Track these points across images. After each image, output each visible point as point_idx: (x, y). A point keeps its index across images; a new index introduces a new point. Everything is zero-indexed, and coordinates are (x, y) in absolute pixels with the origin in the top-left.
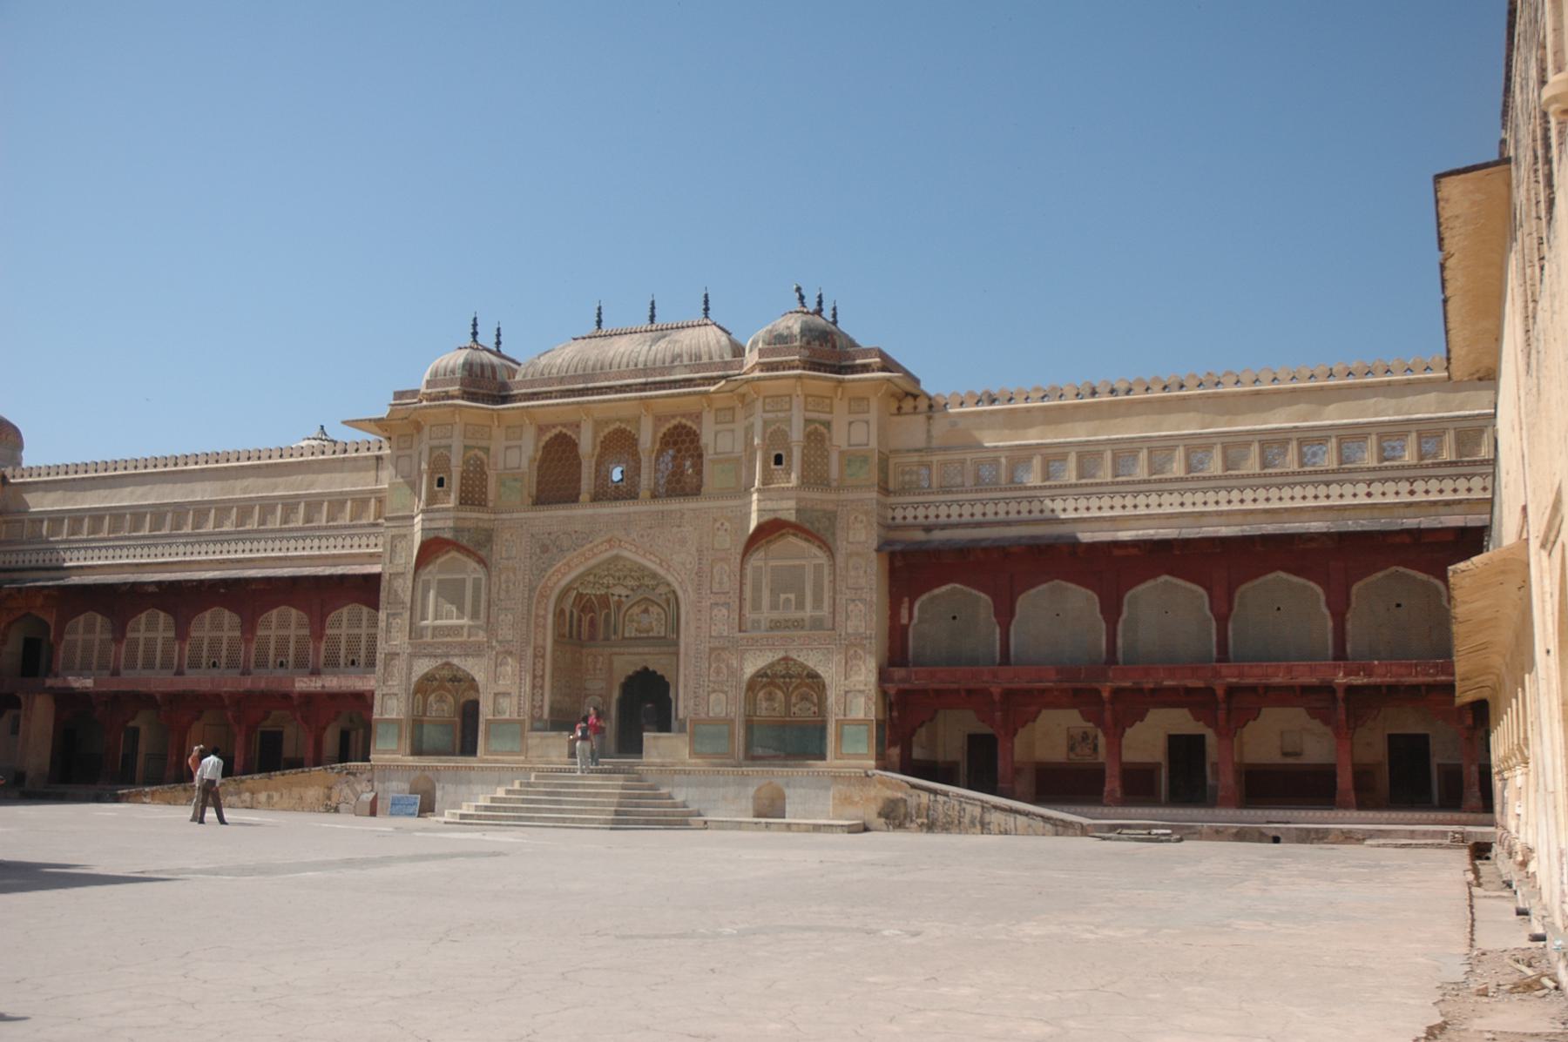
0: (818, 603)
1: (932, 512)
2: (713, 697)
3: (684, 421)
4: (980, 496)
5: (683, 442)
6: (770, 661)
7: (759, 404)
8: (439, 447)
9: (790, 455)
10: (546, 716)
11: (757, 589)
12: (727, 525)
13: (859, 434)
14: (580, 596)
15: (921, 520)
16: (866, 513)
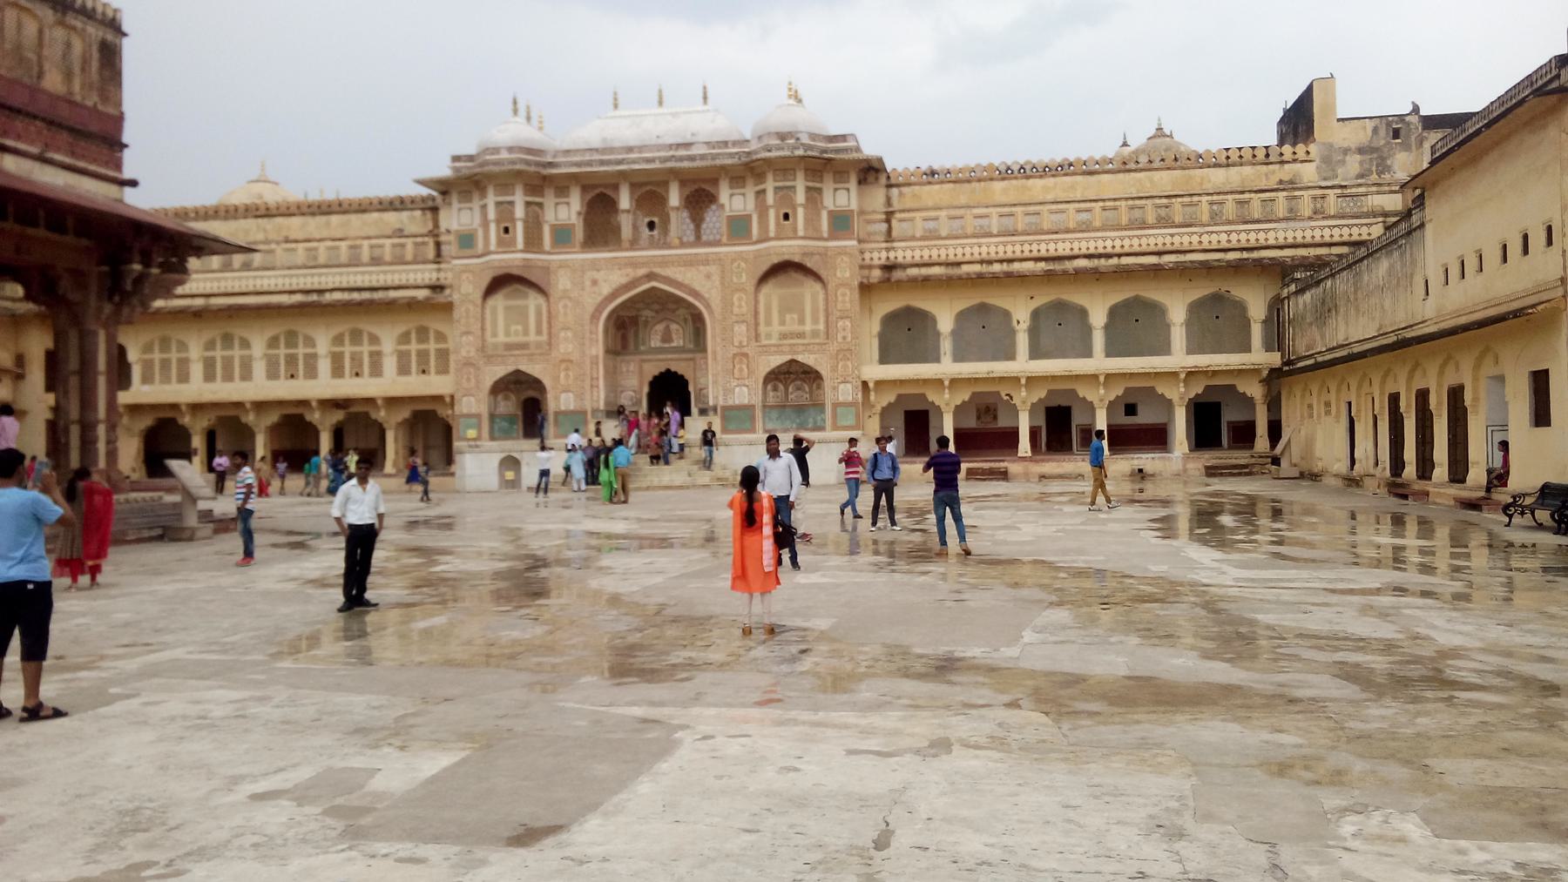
0: (815, 321)
7: (770, 177)
10: (602, 407)
14: (618, 317)
15: (883, 262)
16: (851, 255)
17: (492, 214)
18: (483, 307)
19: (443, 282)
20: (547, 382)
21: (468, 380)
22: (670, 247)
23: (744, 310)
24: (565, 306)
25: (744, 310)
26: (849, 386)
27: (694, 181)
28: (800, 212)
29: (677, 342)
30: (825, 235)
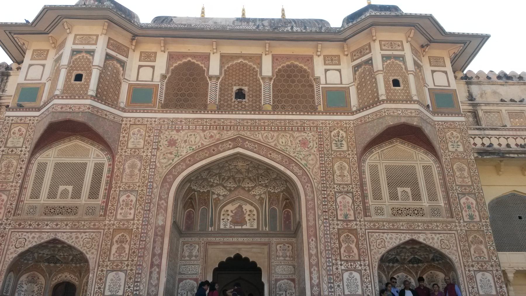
0: (432, 196)
2: (346, 275)
4: (519, 133)
5: (295, 76)
7: (376, 47)
8: (79, 52)
9: (407, 82)
11: (375, 181)
12: (341, 132)
14: (190, 189)
15: (479, 146)
16: (461, 131)
17: (65, 61)
20: (91, 257)
22: (259, 110)
23: (348, 179)
24: (133, 166)
25: (348, 179)
26: (488, 276)
27: (288, 57)
28: (411, 78)
29: (250, 224)
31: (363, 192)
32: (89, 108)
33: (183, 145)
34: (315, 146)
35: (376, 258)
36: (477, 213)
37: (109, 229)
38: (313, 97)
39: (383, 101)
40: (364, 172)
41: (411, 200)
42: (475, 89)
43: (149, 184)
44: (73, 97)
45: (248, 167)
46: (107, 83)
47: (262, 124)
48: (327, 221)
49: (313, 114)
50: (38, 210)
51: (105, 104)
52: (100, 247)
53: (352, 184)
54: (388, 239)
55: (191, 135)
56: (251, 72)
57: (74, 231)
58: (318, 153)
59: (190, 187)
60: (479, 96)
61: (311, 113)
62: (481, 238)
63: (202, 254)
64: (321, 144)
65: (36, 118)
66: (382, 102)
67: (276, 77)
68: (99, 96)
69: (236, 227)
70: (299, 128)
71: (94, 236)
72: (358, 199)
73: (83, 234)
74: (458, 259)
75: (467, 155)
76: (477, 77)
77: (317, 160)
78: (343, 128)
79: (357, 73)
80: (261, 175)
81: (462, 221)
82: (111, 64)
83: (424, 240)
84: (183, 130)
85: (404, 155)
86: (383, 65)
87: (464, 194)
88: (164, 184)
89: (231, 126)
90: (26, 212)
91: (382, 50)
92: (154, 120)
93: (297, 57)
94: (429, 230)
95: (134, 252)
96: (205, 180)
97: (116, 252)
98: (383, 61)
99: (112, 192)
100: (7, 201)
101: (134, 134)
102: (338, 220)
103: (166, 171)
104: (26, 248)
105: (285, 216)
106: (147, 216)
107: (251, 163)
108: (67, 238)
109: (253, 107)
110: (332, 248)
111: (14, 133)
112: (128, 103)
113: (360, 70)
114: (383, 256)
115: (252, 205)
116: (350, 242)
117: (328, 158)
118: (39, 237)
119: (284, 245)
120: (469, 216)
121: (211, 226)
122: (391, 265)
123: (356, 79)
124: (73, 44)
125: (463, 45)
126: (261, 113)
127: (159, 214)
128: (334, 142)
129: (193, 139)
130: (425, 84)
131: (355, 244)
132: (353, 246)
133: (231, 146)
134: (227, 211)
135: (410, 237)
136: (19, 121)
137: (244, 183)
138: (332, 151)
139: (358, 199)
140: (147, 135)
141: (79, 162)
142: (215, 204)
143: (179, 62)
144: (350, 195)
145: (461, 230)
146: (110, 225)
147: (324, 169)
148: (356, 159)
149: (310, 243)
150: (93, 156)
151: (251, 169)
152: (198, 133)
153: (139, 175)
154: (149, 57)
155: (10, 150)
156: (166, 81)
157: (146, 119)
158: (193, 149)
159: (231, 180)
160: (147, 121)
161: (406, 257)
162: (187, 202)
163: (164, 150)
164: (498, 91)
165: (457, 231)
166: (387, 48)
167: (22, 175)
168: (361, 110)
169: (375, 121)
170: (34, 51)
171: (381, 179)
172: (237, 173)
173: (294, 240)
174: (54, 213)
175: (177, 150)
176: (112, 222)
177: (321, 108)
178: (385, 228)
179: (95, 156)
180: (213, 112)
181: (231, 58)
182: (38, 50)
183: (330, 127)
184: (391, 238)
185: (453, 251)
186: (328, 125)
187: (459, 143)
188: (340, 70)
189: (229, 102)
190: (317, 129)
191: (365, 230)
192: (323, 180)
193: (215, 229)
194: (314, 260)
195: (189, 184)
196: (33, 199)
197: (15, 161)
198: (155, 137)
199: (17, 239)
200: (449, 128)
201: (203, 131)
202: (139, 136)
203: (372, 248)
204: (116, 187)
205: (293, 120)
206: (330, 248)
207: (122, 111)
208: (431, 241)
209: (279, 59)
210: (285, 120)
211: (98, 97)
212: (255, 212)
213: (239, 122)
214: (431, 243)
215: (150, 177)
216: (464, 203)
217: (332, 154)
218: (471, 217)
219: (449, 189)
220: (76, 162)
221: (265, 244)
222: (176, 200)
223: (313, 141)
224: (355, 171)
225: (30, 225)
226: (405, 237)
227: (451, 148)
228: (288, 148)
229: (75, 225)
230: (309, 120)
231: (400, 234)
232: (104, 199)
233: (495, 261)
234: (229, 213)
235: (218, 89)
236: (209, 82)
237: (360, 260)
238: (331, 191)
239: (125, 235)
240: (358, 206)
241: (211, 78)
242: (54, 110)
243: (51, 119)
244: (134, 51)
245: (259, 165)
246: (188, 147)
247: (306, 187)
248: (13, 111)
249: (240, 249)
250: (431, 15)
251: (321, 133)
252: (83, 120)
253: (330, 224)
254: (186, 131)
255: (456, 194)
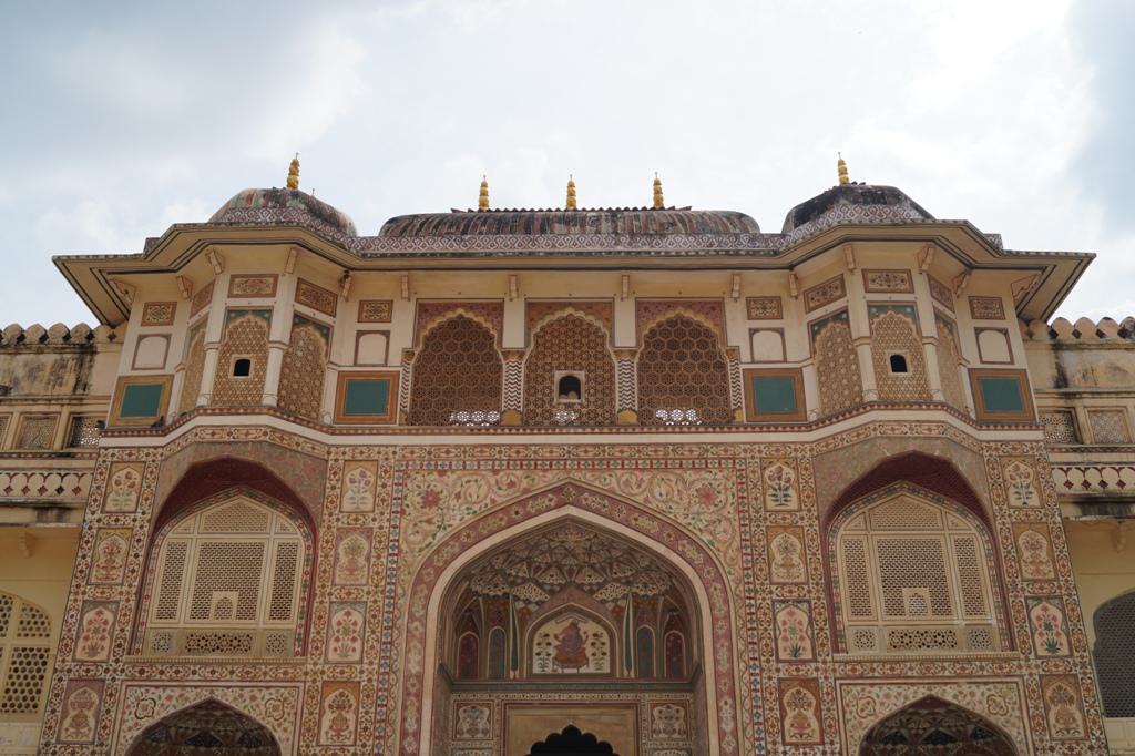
0: (974, 605)
1: (1093, 477)
3: (689, 314)
5: (687, 344)
6: (900, 704)
7: (855, 285)
8: (241, 312)
11: (858, 575)
13: (994, 350)
15: (1078, 489)
16: (1035, 462)
17: (214, 332)
18: (152, 543)
19: (67, 497)
21: (79, 722)
22: (612, 425)
24: (354, 550)
27: (670, 305)
28: (930, 353)
30: (973, 416)
31: (831, 600)
32: (265, 434)
33: (453, 503)
34: (730, 501)
35: (856, 737)
36: (1064, 639)
37: (314, 681)
38: (724, 391)
39: (871, 404)
40: (833, 556)
41: (930, 612)
42: (1071, 361)
43: (388, 587)
44: (233, 411)
45: (588, 543)
46: (297, 375)
47: (618, 454)
48: (757, 663)
49: (726, 430)
50: (174, 642)
51: (294, 422)
52: (299, 717)
53: (807, 583)
54: (881, 696)
55: (469, 482)
56: (592, 337)
57: (248, 684)
58: (737, 518)
59: (468, 589)
60: (1079, 375)
61: (722, 428)
62: (1071, 692)
63: (497, 726)
64: (743, 497)
65: (160, 450)
66: (868, 408)
67: (646, 349)
68: (282, 404)
69: (567, 671)
70: (696, 461)
71: (286, 694)
72: (820, 614)
73: (264, 691)
74: (1023, 735)
75: (1046, 515)
76: (1077, 334)
77: (734, 530)
78: (790, 461)
79: (818, 337)
80: (617, 560)
81: (1032, 656)
82: (303, 334)
83: (955, 697)
84: (453, 472)
85: (916, 518)
86: (870, 325)
87: (1038, 599)
88: (418, 588)
89: (551, 461)
90: (151, 645)
91: (866, 292)
92: (392, 449)
93: (689, 305)
94: (966, 677)
95: (366, 729)
96: (501, 572)
97: (331, 728)
98: (871, 316)
99: (315, 605)
100: (114, 624)
101: (352, 481)
102: (778, 660)
103: (420, 560)
104: (157, 718)
105: (670, 644)
106: (388, 655)
107: (596, 536)
108: (235, 699)
109: (596, 415)
110: (766, 720)
111: (118, 483)
112: (339, 415)
113: (823, 331)
114: (872, 731)
115: (598, 623)
116: (802, 707)
117: (758, 526)
118: (181, 696)
119: (669, 707)
120: (1049, 645)
121: (514, 669)
122: (889, 747)
123: (815, 352)
124: (229, 297)
125: (1040, 272)
126: (614, 431)
127: (410, 650)
128: (771, 492)
129: (473, 489)
130: (961, 361)
131: (813, 709)
132: (810, 713)
133: (553, 504)
134: (547, 635)
135: (927, 692)
136: (126, 457)
137: (581, 576)
138: (766, 511)
139: (820, 614)
140: (379, 483)
141: (248, 541)
142: (520, 622)
143: (440, 320)
144: (805, 606)
145: (1031, 675)
146: (315, 673)
147: (749, 551)
148: (817, 528)
149: (721, 708)
150: (276, 532)
151: (594, 548)
152: (484, 477)
153: (366, 569)
154: (376, 311)
155: (113, 518)
156: (412, 362)
157: (376, 449)
158: (475, 512)
159: (553, 571)
160: (379, 453)
161: (921, 732)
162: (463, 616)
163: (414, 514)
164: (1120, 365)
165: (1022, 676)
166: (879, 287)
167: (139, 570)
168: (827, 422)
169: (856, 447)
170: (147, 306)
171: (868, 569)
172: (566, 556)
173: (688, 696)
174: (205, 649)
175: (443, 515)
176: (319, 667)
177: (741, 416)
178: (876, 674)
179: (278, 529)
180: (514, 431)
181: (550, 308)
182: (154, 304)
183: (761, 458)
184: (887, 696)
185: (1013, 720)
186: (757, 455)
187: (1031, 489)
188: (782, 329)
189: (547, 407)
190: (734, 463)
191: (835, 679)
192: (748, 576)
193: (521, 674)
194: (729, 744)
195: (467, 583)
196: (163, 620)
197: (121, 541)
198: (395, 487)
199: (138, 700)
200: (1011, 456)
201: (495, 472)
202: (362, 485)
203: (848, 716)
204: (323, 595)
205: (682, 445)
206: (761, 720)
207: (327, 432)
208: (968, 698)
209: (651, 308)
210: (665, 445)
211: (280, 410)
212: (605, 639)
213: (569, 452)
214: (968, 704)
215: (389, 573)
216: (1038, 618)
217: (765, 519)
218: (1052, 647)
219: (1008, 589)
220: (243, 541)
221: (628, 706)
222: (442, 619)
223: (726, 489)
224: (814, 554)
225: (162, 672)
226: (916, 692)
227: (1013, 501)
228: (674, 506)
229: (248, 673)
230: (717, 445)
231: (906, 687)
232: (301, 618)
233: (1098, 739)
234: (551, 639)
235: (522, 378)
236: (503, 362)
237: (823, 743)
238: (764, 599)
239: (346, 692)
240: (821, 629)
241: (507, 354)
242: (198, 439)
243: (194, 457)
244: (347, 300)
245: (613, 541)
246: (464, 507)
247: (712, 589)
248: (113, 436)
249: (575, 717)
250: (965, 222)
251: (744, 473)
252: (257, 460)
253: (762, 670)
254: (458, 472)
255: (1023, 600)
